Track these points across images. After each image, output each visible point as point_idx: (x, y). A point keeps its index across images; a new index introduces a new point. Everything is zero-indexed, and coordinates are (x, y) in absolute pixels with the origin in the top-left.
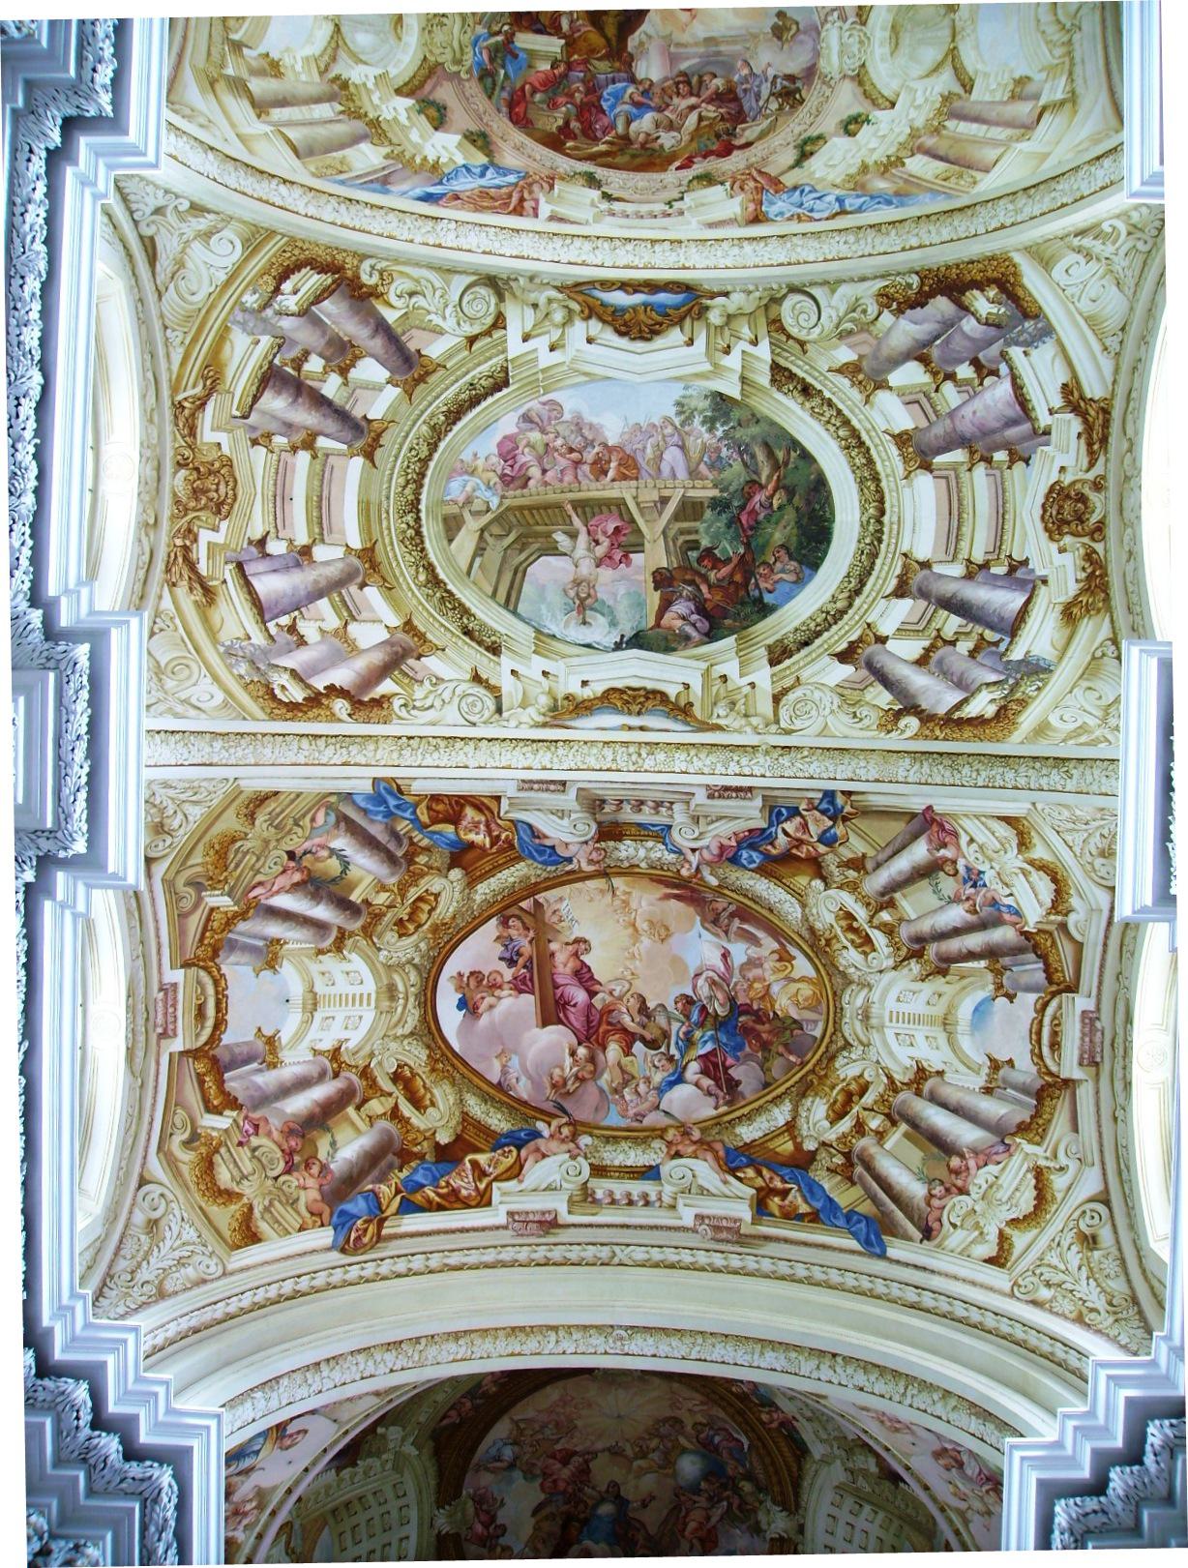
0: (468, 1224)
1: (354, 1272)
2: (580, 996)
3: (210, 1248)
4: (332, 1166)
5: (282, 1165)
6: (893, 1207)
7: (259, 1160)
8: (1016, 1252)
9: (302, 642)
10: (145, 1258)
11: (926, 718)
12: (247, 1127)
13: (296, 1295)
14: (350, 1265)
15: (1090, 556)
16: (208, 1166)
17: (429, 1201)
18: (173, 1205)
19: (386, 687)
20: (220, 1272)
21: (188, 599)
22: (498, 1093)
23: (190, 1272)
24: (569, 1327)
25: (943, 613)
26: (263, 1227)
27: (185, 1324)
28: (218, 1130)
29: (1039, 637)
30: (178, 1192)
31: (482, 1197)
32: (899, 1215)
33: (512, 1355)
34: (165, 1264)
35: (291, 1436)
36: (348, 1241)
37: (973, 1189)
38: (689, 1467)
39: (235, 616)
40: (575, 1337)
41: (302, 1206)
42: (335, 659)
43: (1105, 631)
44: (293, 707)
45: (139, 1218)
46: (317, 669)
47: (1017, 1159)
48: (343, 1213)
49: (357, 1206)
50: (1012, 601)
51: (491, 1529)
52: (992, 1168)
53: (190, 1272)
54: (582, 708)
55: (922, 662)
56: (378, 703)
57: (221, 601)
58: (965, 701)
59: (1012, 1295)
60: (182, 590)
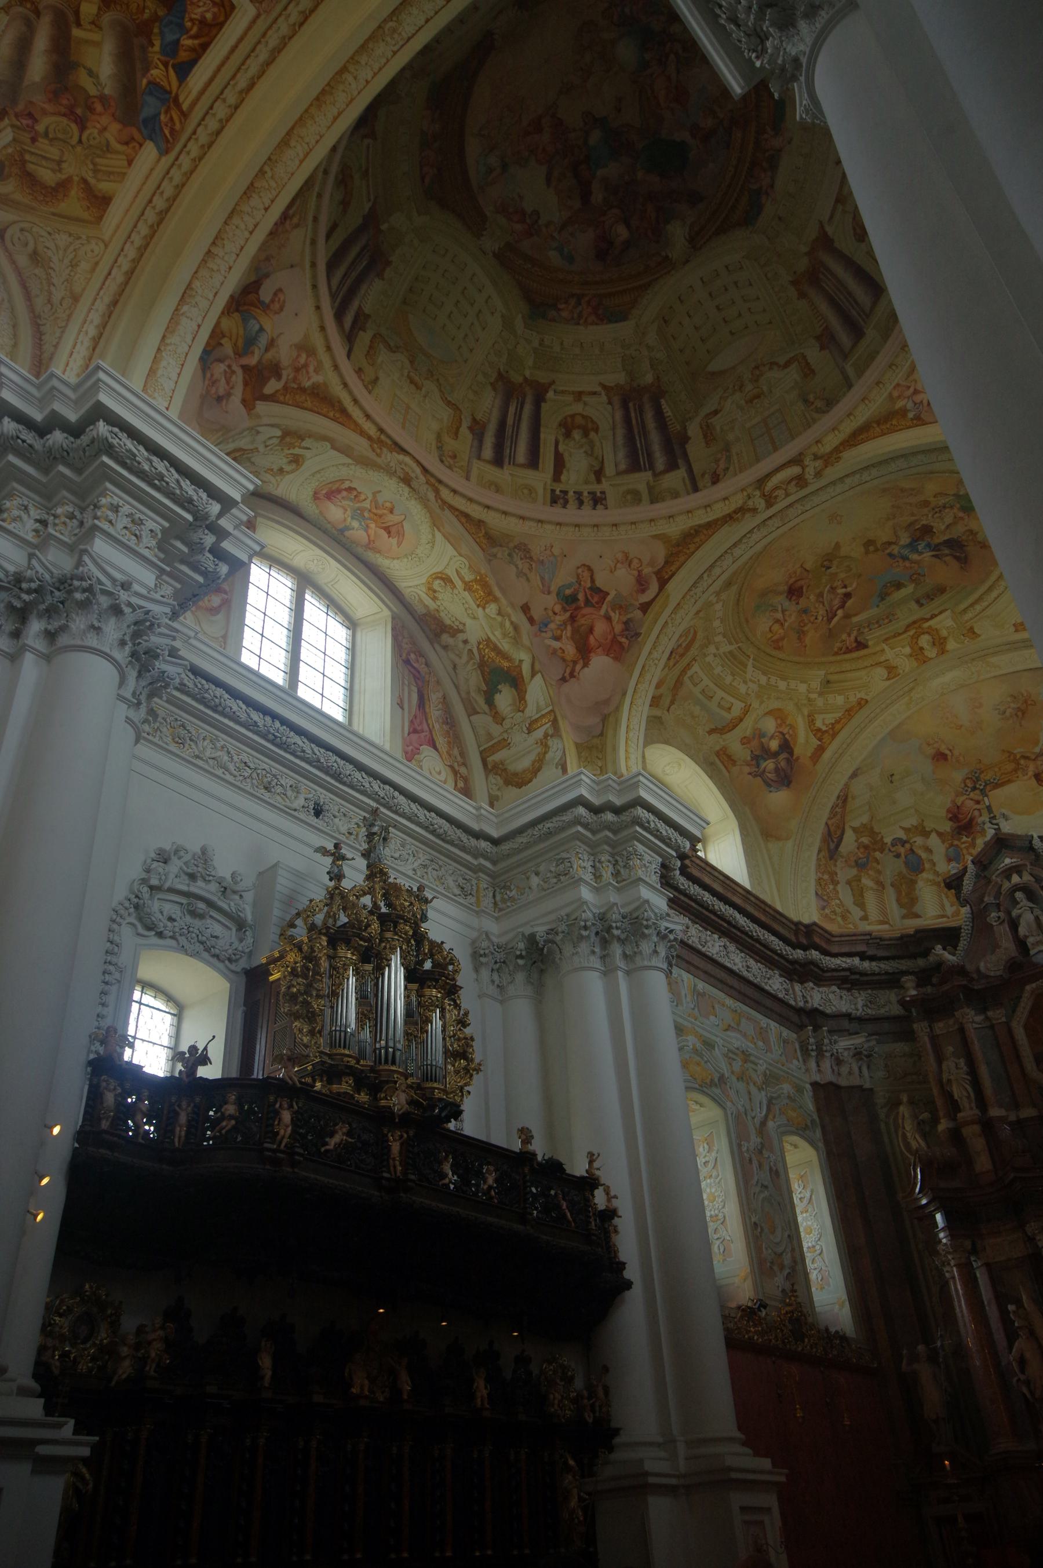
0: (232, 42)
1: (185, 162)
3: (84, 237)
4: (107, 91)
5: (74, 126)
7: (56, 139)
12: (24, 122)
13: (163, 215)
14: (177, 159)
16: (30, 180)
17: (192, 49)
18: (34, 230)
20: (102, 246)
23: (84, 266)
24: (352, 58)
26: (104, 187)
27: (101, 306)
28: (8, 145)
31: (223, 6)
33: (335, 119)
35: (272, 301)
36: (168, 141)
38: (626, 52)
40: (363, 62)
41: (115, 145)
45: (23, 260)
48: (145, 122)
49: (150, 106)
51: (528, 221)
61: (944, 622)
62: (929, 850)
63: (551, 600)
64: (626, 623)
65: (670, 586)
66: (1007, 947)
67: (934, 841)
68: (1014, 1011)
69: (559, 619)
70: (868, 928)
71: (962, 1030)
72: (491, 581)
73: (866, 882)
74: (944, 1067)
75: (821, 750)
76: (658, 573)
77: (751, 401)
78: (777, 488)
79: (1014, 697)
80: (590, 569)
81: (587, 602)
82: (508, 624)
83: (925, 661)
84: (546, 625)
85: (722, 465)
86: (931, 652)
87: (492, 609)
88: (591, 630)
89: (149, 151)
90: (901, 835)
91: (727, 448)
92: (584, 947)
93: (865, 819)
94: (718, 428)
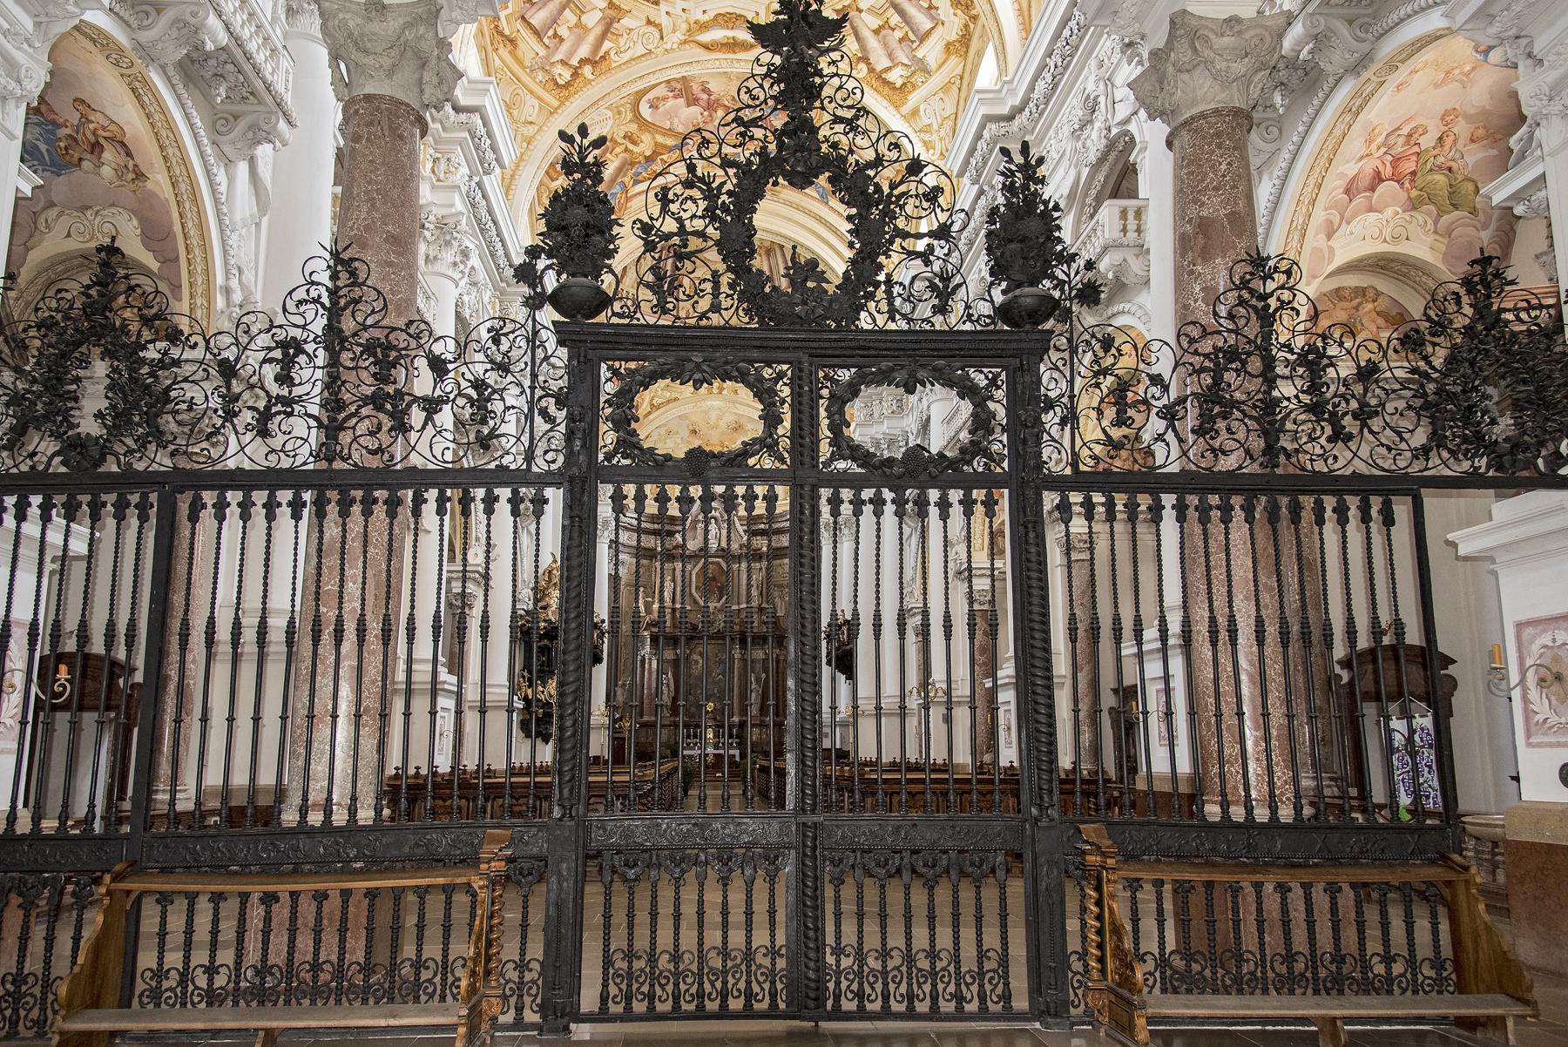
2: (705, 96)
9: (562, 40)
11: (871, 70)
15: (966, 26)
19: (607, 45)
21: (504, 52)
22: (670, 132)
25: (892, 10)
29: (931, 51)
39: (530, 46)
42: (579, 41)
43: (959, 71)
44: (568, 85)
46: (571, 54)
50: (927, 25)
54: (703, 27)
55: (876, 32)
56: (603, 58)
57: (521, 44)
58: (889, 69)
60: (502, 51)
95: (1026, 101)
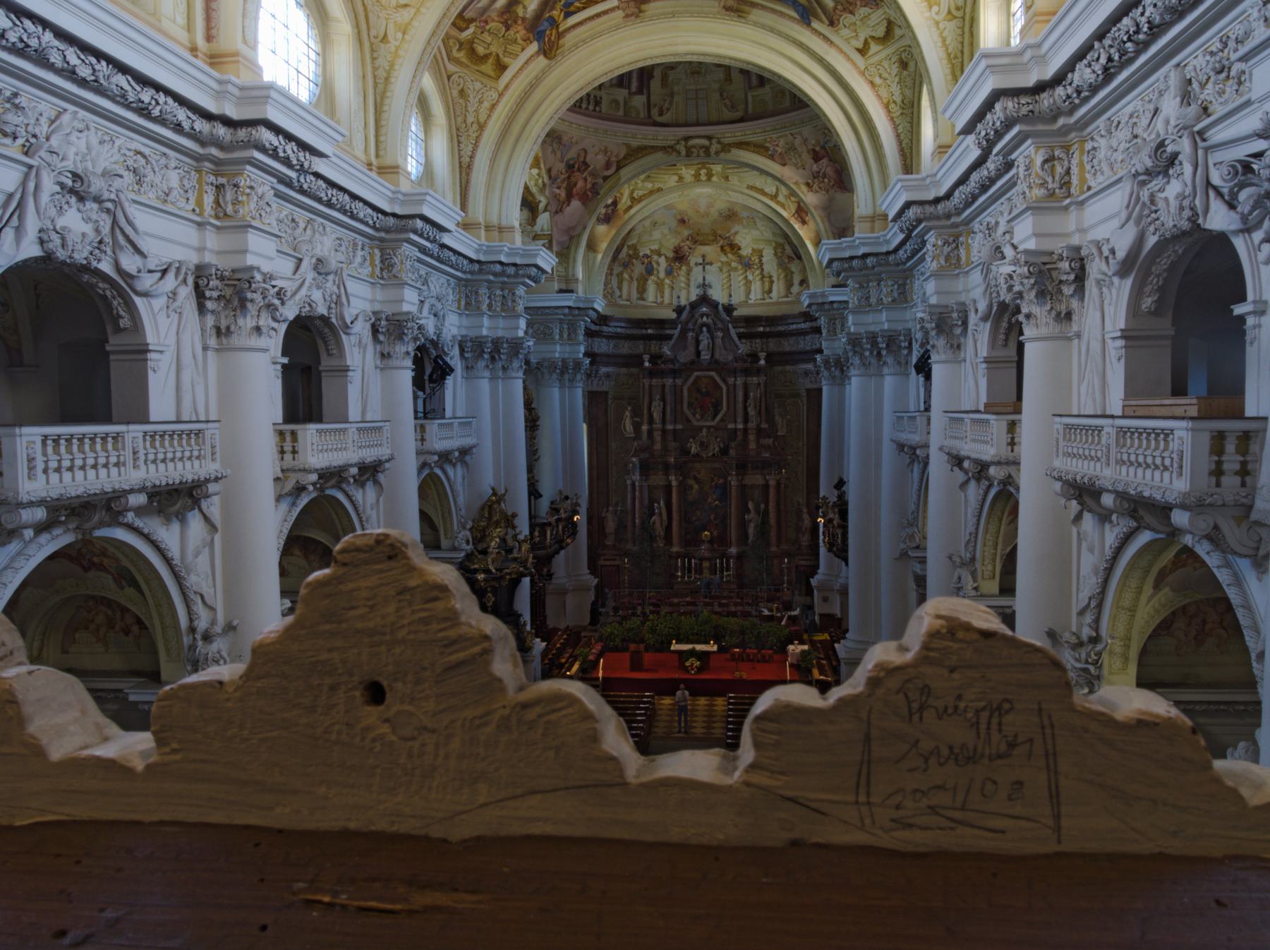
4: (528, 16)
6: (816, 5)
8: (871, 52)
10: (467, 111)
16: (472, 52)
26: (506, 60)
30: (466, 71)
32: (819, 11)
34: (474, 108)
37: (857, 15)
45: (455, 93)
47: (880, 12)
48: (538, 33)
52: (867, 9)
53: (487, 104)
59: (862, 74)
61: (717, 168)
62: (658, 264)
63: (561, 166)
64: (594, 185)
65: (623, 172)
66: (692, 349)
67: (662, 260)
68: (686, 380)
69: (563, 176)
70: (622, 302)
71: (664, 386)
72: (542, 161)
73: (626, 276)
74: (654, 403)
75: (630, 207)
76: (618, 162)
77: (693, 73)
78: (694, 147)
79: (729, 210)
80: (585, 151)
81: (579, 170)
82: (540, 181)
83: (699, 180)
84: (556, 180)
85: (666, 105)
86: (703, 178)
87: (535, 171)
88: (576, 184)
89: (534, 47)
90: (648, 252)
91: (672, 95)
92: (554, 376)
93: (634, 241)
94: (671, 78)
95: (1059, 79)
